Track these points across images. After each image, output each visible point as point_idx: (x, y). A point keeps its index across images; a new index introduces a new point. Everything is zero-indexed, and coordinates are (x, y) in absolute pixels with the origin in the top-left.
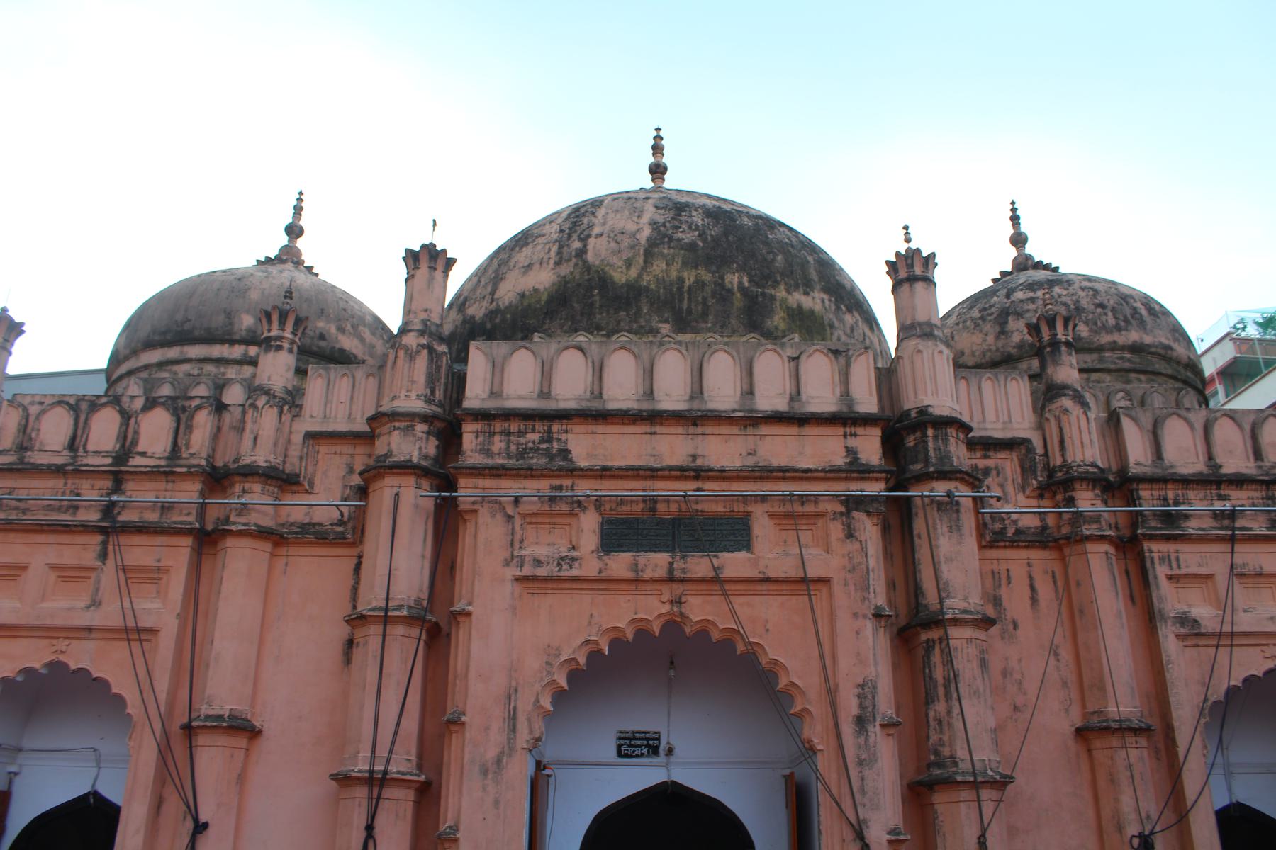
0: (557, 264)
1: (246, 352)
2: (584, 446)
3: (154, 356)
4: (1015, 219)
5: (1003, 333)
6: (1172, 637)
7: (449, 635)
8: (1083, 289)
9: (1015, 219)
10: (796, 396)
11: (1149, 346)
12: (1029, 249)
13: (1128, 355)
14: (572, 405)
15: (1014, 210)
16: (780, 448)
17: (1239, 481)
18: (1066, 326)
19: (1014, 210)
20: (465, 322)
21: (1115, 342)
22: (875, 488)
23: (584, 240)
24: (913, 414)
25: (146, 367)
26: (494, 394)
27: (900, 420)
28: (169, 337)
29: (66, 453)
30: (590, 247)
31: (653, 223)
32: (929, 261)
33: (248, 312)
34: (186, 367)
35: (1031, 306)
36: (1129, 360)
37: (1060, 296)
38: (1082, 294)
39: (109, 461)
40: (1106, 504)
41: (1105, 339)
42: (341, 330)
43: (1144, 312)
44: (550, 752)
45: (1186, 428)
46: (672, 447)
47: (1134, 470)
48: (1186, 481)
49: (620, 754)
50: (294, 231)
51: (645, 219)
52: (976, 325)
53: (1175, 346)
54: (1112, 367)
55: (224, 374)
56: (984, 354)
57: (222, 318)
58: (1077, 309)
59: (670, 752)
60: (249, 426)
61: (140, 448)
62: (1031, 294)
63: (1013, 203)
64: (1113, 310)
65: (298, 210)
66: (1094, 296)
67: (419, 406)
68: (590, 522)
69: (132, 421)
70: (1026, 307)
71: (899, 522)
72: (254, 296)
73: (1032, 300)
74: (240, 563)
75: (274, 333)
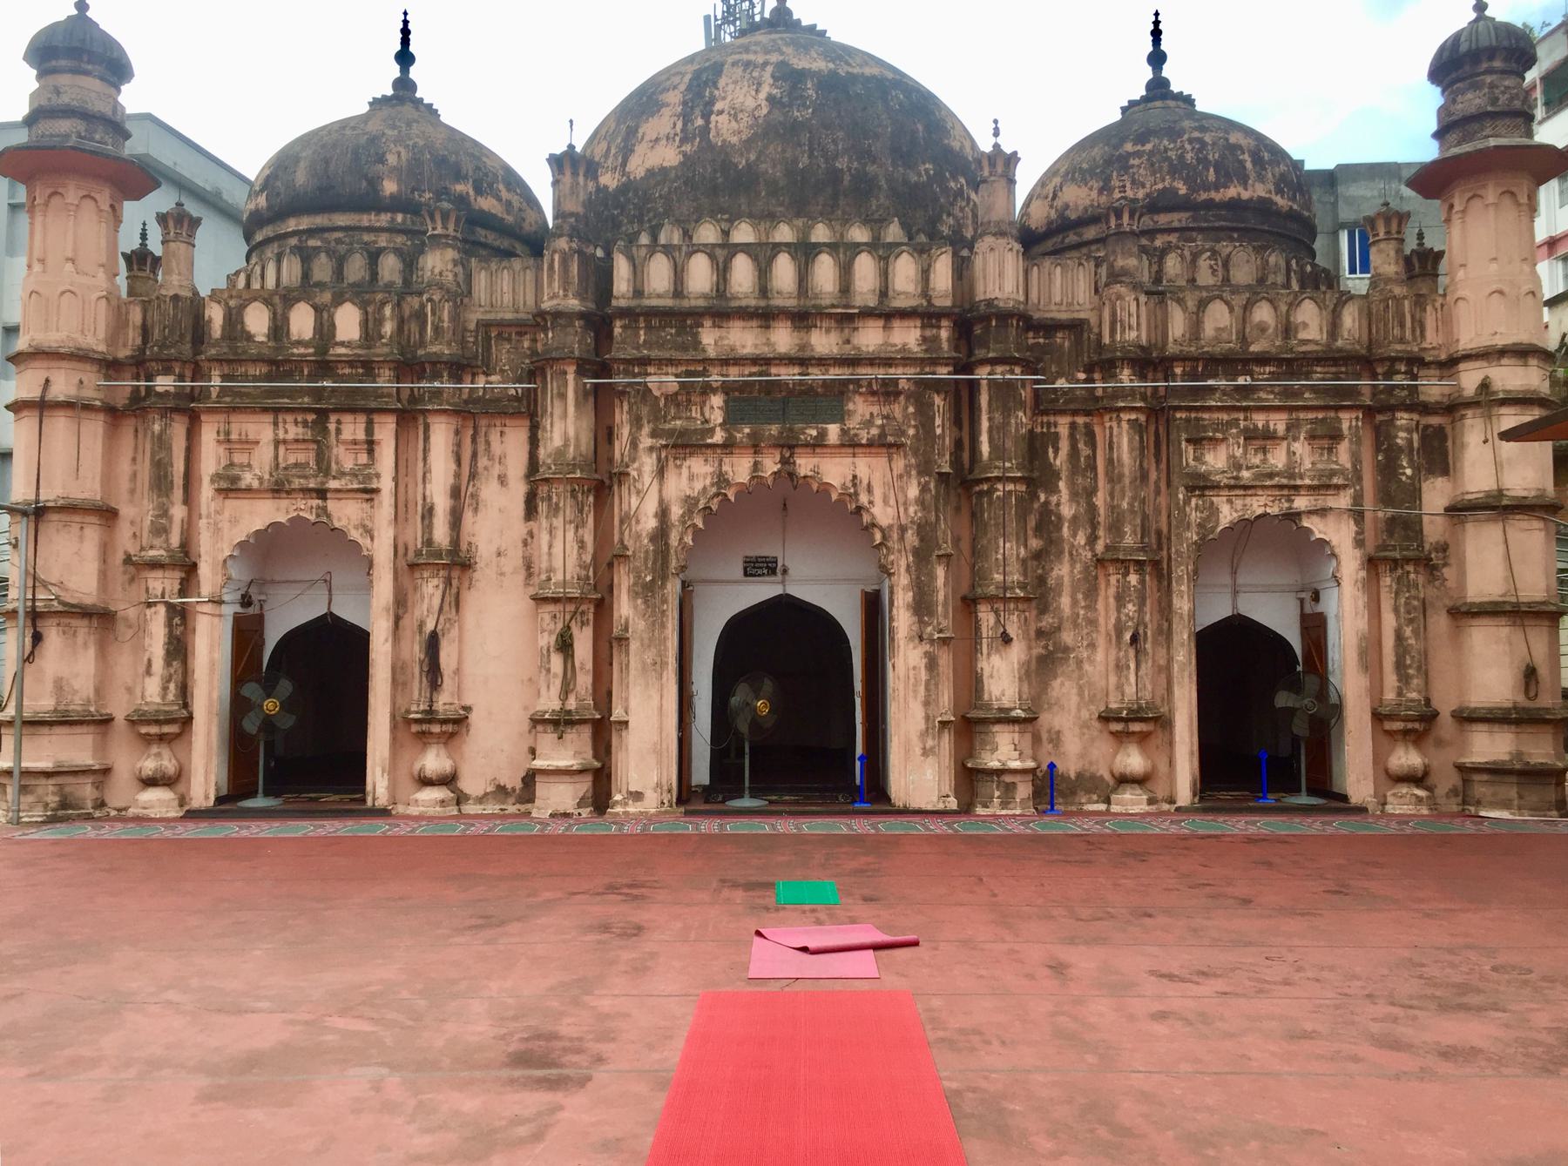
0: (683, 141)
1: (393, 220)
2: (709, 337)
3: (305, 223)
4: (1156, 34)
5: (1106, 188)
6: (1182, 489)
7: (610, 487)
8: (1190, 141)
9: (1156, 34)
10: (884, 293)
12: (1167, 71)
14: (701, 303)
15: (1157, 23)
16: (870, 338)
17: (1263, 360)
18: (1131, 216)
19: (1157, 23)
20: (598, 189)
21: (1212, 200)
22: (943, 373)
23: (706, 116)
24: (982, 307)
25: (294, 233)
26: (638, 293)
27: (971, 310)
30: (712, 125)
31: (771, 99)
32: (1012, 160)
35: (1136, 162)
37: (1166, 150)
38: (1188, 147)
39: (311, 350)
40: (1143, 378)
41: (1204, 196)
42: (479, 191)
43: (1249, 165)
44: (690, 574)
45: (1225, 308)
46: (783, 339)
47: (1172, 349)
49: (746, 574)
50: (405, 57)
51: (763, 95)
53: (1278, 199)
55: (375, 242)
56: (1086, 209)
57: (364, 184)
59: (785, 571)
61: (340, 337)
62: (1139, 147)
64: (1218, 167)
65: (406, 32)
66: (1200, 150)
67: (573, 304)
68: (717, 400)
69: (325, 315)
71: (963, 399)
73: (1138, 154)
74: (441, 434)
75: (439, 231)
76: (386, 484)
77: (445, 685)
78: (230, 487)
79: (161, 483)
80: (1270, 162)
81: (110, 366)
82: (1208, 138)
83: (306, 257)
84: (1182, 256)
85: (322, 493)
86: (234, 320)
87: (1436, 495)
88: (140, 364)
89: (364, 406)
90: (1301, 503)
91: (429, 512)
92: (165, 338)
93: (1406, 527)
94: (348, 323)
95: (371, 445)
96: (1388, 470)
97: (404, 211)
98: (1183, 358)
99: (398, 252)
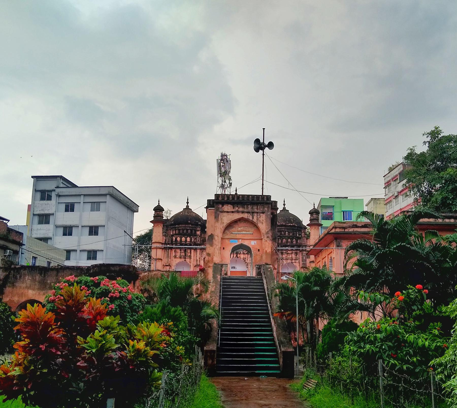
74: (198, 251)
76: (192, 257)
78: (175, 257)
79: (168, 257)
81: (162, 244)
83: (179, 230)
85: (185, 258)
86: (176, 239)
87: (308, 261)
88: (165, 244)
89: (191, 249)
90: (293, 261)
91: (197, 261)
93: (305, 264)
94: (188, 239)
95: (191, 253)
96: (302, 258)
99: (190, 229)
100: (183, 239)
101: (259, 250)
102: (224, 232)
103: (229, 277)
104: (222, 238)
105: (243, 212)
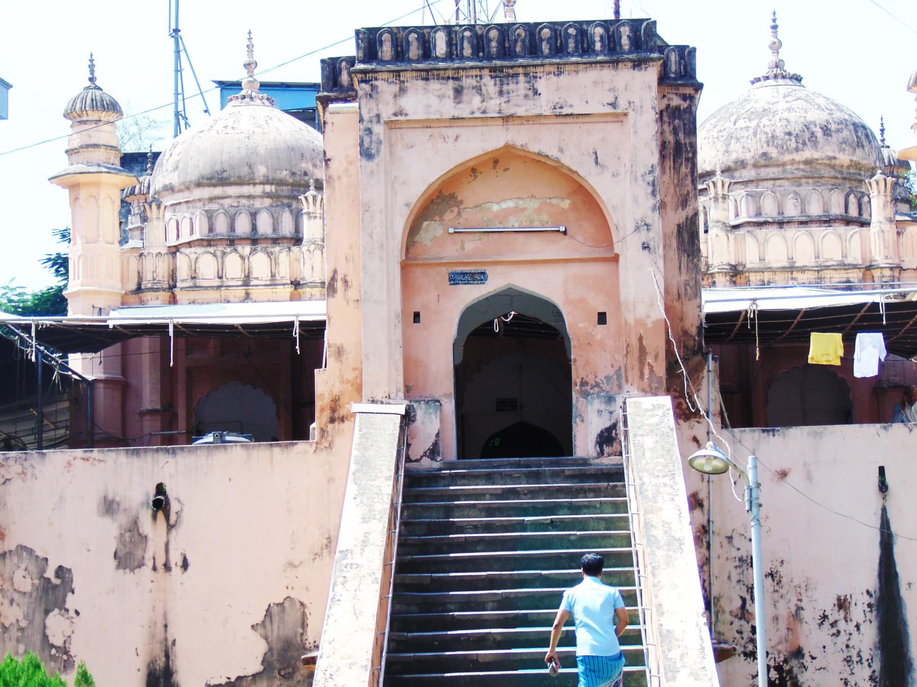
1: (263, 192)
3: (206, 192)
11: (817, 159)
13: (802, 166)
17: (803, 270)
28: (213, 181)
29: (217, 279)
33: (261, 163)
34: (227, 202)
35: (746, 134)
36: (803, 170)
38: (779, 124)
41: (787, 157)
48: (773, 271)
52: (714, 143)
54: (790, 176)
57: (246, 168)
58: (773, 137)
60: (308, 262)
61: (254, 275)
63: (774, 14)
65: (250, 47)
66: (786, 126)
69: (246, 260)
70: (743, 134)
72: (262, 150)
73: (747, 128)
75: (311, 210)
77: (418, 417)
80: (838, 131)
82: (792, 116)
83: (210, 216)
84: (775, 198)
92: (154, 279)
97: (272, 184)
98: (756, 271)
100: (233, 265)
101: (602, 318)
102: (414, 229)
103: (450, 466)
104: (406, 267)
105: (507, 119)
